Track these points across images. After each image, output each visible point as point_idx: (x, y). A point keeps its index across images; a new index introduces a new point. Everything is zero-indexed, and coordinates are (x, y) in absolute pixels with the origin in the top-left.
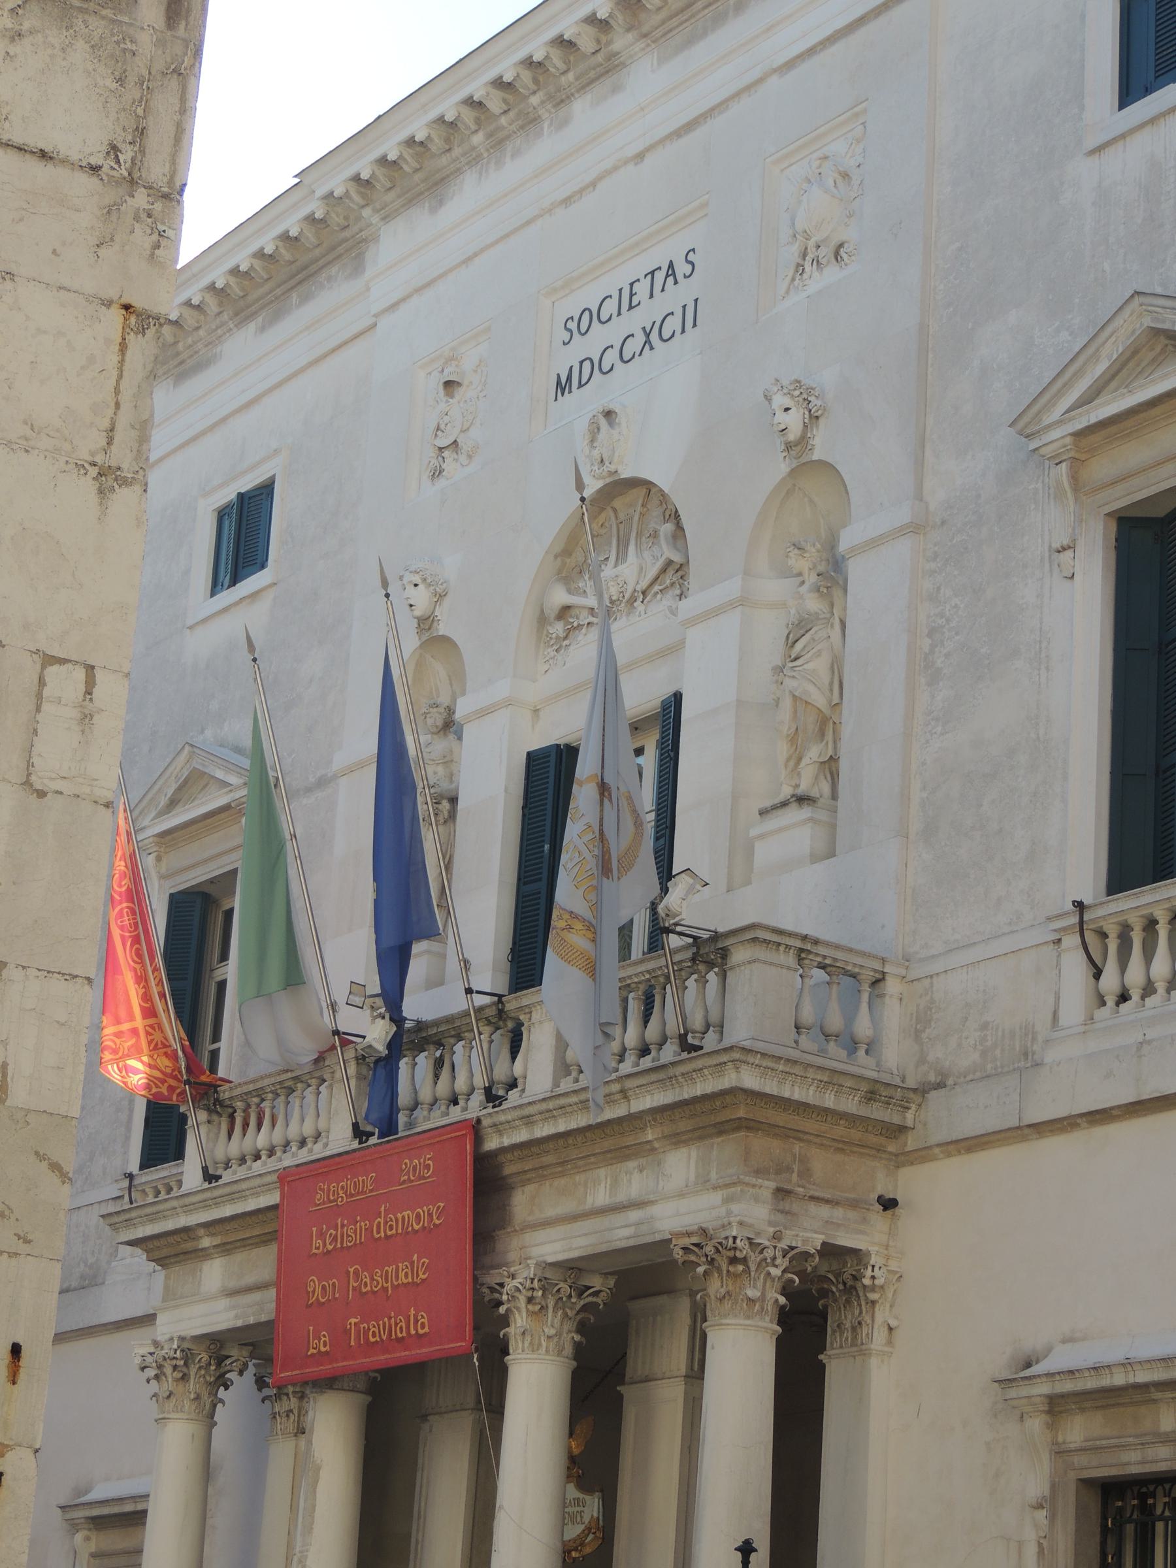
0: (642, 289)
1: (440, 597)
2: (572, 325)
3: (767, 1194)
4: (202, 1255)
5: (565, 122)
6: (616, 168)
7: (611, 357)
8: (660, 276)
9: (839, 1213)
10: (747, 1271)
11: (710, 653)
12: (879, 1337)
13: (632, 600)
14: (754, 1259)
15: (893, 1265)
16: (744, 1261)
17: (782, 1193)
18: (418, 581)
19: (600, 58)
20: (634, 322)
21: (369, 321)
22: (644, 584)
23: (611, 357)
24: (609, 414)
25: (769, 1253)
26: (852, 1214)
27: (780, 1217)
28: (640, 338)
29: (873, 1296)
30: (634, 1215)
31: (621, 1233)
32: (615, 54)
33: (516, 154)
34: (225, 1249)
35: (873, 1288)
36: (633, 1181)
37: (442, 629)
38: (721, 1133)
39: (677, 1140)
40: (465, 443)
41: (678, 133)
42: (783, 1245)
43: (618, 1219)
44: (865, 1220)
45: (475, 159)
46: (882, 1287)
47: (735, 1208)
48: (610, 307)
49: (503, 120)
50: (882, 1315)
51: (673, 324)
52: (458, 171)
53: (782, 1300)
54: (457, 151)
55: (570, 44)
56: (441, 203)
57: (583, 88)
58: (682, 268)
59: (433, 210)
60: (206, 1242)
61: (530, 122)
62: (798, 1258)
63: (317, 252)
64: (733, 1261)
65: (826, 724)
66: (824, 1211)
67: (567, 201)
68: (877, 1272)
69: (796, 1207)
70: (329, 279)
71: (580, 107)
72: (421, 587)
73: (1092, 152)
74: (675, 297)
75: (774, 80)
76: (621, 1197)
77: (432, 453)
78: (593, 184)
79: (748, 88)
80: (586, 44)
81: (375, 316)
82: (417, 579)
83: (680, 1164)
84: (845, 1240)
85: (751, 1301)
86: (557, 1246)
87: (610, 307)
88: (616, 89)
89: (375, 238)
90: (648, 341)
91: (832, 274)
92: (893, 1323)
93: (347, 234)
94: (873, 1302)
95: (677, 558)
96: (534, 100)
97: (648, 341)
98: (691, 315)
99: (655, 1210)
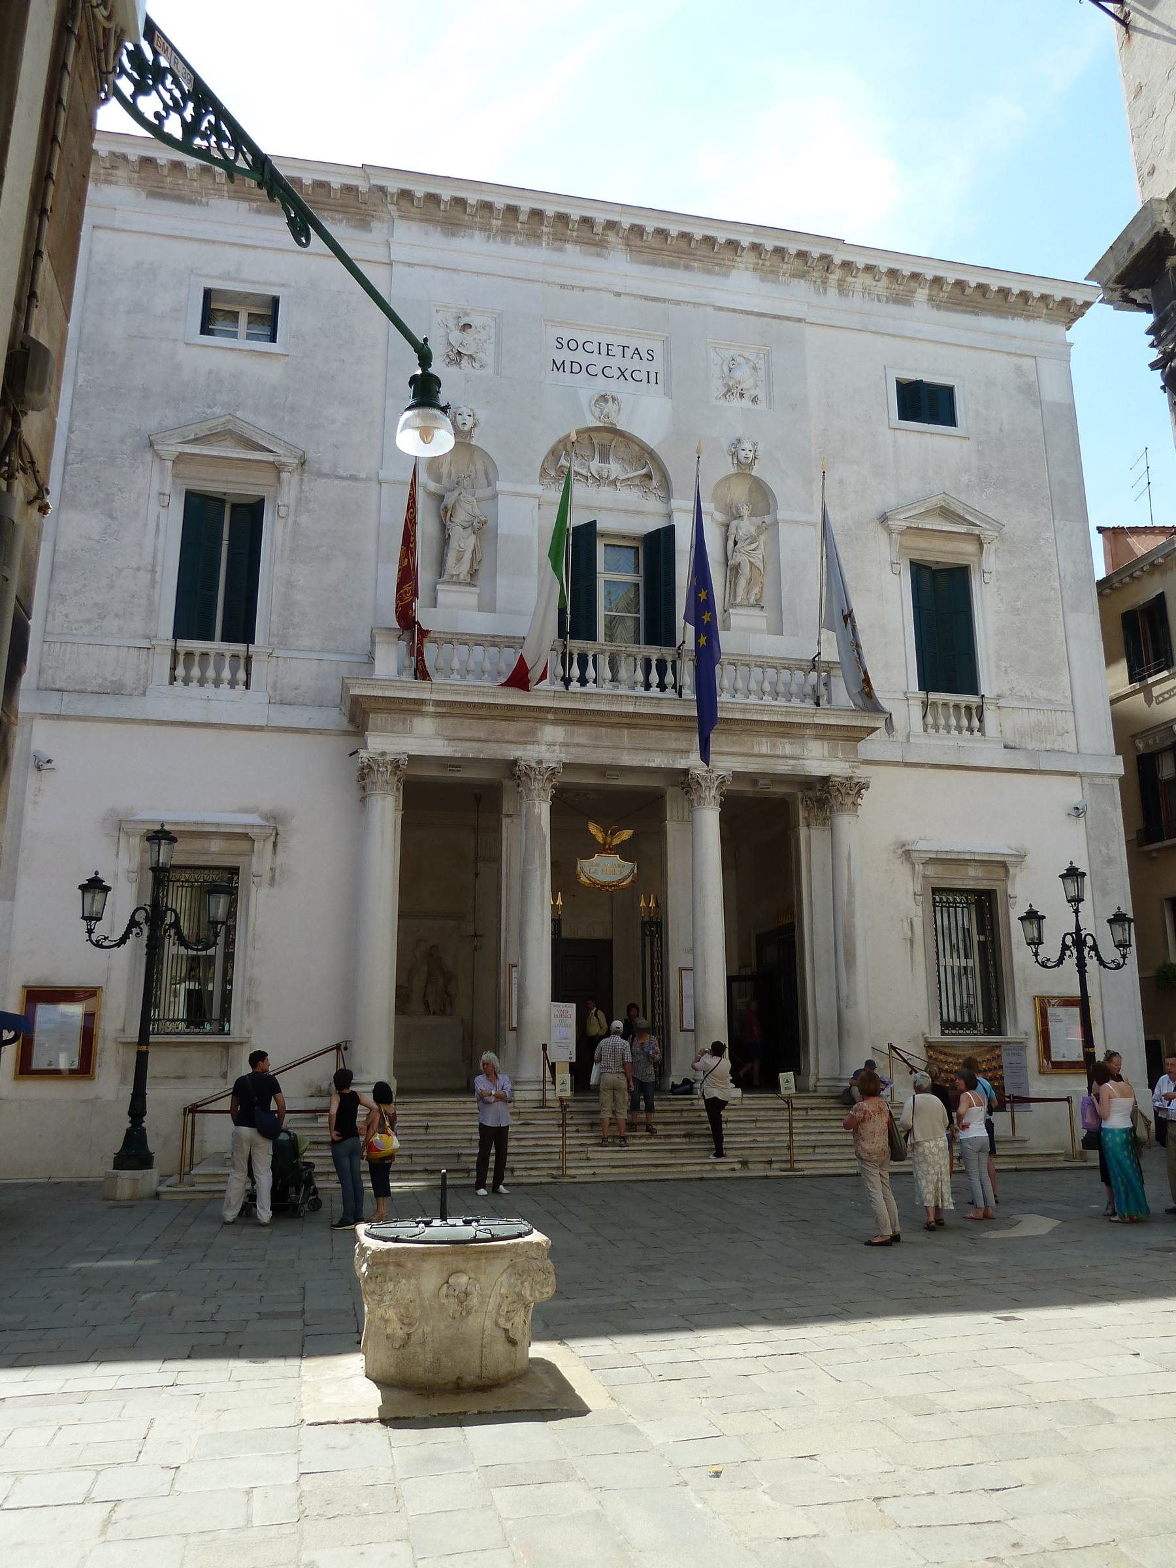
31: (783, 767)
39: (817, 737)
41: (646, 298)
43: (780, 761)
45: (486, 228)
49: (519, 225)
54: (478, 219)
57: (576, 242)
60: (431, 709)
67: (562, 286)
71: (569, 247)
75: (710, 310)
80: (598, 229)
86: (737, 765)
93: (363, 206)
96: (545, 229)
99: (806, 762)
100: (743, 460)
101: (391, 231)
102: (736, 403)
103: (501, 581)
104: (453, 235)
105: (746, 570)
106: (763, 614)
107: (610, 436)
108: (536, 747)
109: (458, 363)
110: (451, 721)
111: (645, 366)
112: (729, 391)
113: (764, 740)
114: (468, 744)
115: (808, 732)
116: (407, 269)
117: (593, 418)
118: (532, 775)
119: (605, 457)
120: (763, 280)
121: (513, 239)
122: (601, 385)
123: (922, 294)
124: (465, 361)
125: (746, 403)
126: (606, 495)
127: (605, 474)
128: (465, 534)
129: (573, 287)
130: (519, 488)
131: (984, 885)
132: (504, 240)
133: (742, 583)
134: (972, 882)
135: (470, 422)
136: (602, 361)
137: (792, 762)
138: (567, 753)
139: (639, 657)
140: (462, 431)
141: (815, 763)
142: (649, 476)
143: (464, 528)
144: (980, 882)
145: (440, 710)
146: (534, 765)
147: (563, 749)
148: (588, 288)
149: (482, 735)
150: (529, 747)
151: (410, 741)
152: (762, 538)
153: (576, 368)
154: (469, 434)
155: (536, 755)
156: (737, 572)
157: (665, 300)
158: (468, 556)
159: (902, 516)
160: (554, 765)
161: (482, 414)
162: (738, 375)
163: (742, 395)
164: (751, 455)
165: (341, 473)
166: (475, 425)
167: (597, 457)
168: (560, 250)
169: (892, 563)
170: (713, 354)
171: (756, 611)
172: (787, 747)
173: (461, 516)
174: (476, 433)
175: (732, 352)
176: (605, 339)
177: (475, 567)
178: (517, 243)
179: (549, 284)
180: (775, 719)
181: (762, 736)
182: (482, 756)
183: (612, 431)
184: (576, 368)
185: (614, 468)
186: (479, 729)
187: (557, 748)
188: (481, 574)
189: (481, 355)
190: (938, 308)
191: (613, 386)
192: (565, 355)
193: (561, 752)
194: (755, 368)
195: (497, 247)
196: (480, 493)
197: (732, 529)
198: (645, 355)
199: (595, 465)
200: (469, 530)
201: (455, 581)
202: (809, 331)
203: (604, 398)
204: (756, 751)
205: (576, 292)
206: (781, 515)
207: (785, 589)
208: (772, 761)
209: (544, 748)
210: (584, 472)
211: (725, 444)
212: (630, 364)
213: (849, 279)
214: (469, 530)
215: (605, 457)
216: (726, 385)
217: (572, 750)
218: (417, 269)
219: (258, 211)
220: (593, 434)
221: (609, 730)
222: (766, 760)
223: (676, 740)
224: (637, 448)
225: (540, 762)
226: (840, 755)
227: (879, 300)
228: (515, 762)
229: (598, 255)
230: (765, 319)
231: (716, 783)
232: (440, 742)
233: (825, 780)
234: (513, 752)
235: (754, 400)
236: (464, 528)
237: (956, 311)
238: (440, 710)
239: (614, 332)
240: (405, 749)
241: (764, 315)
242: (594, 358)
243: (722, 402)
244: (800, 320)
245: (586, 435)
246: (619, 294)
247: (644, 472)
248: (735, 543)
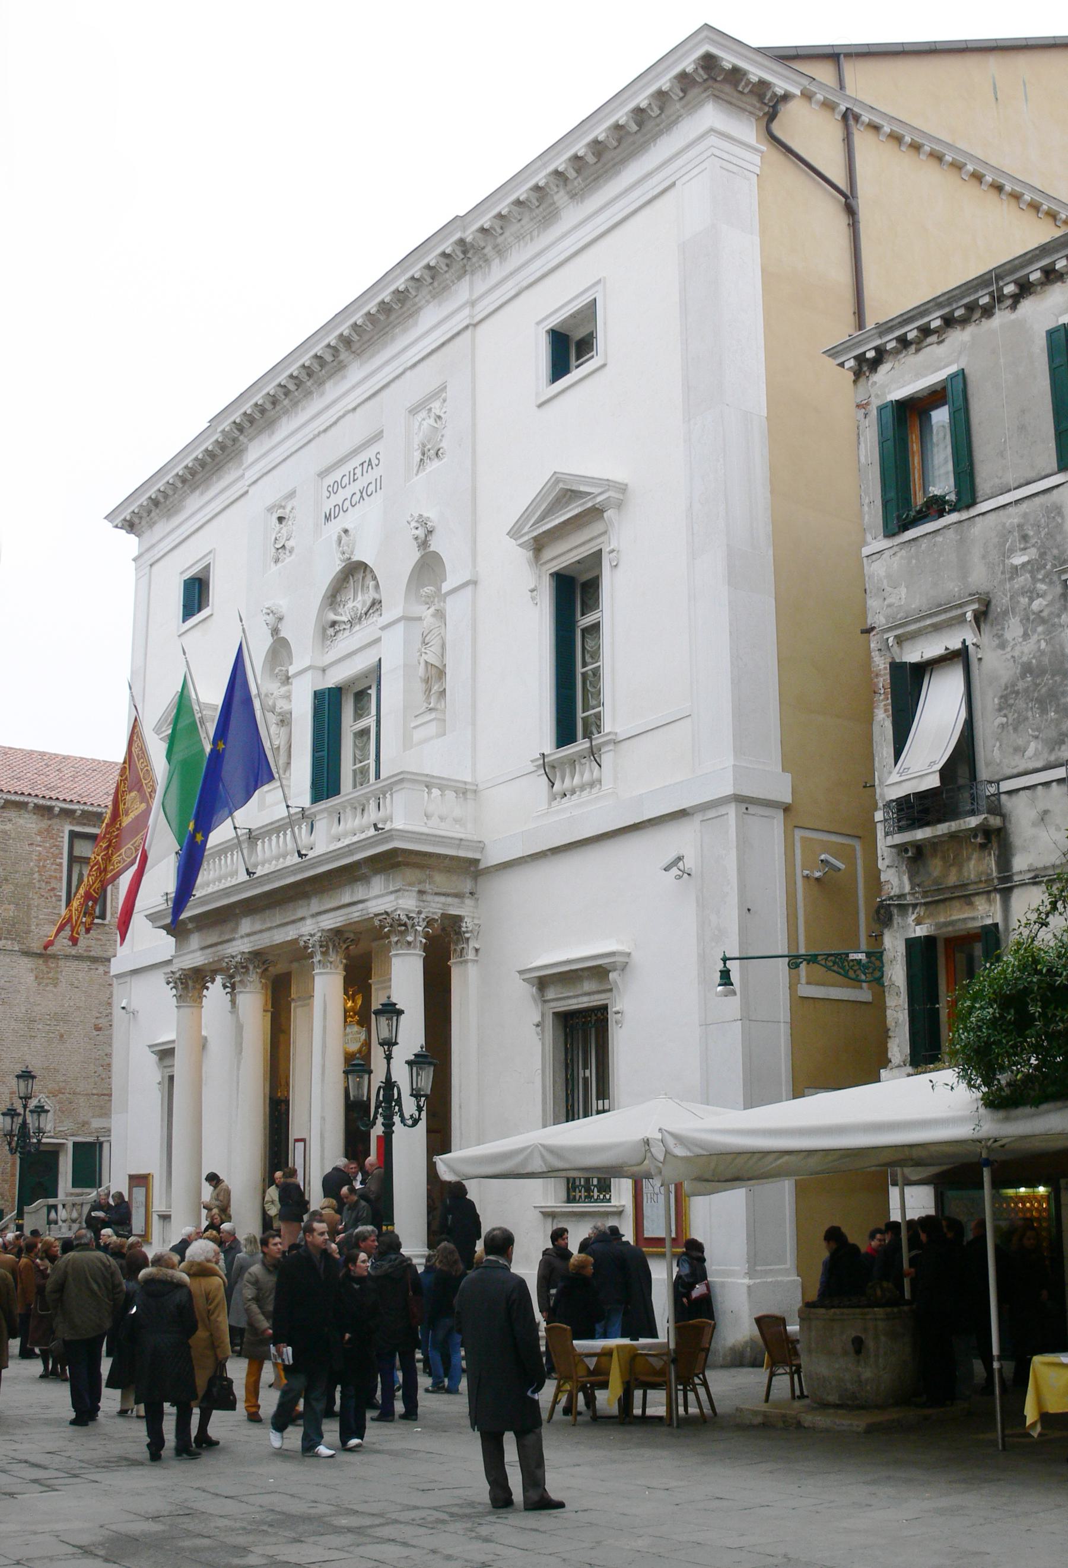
0: (358, 471)
1: (280, 619)
2: (330, 489)
3: (415, 894)
5: (323, 394)
6: (344, 416)
7: (347, 504)
8: (365, 465)
9: (449, 900)
10: (407, 930)
11: (386, 645)
12: (471, 955)
13: (360, 619)
14: (409, 923)
15: (476, 922)
16: (405, 925)
17: (421, 892)
19: (335, 363)
20: (356, 487)
22: (365, 609)
23: (347, 504)
24: (346, 531)
25: (416, 921)
26: (456, 900)
27: (422, 904)
28: (358, 494)
29: (467, 935)
30: (360, 906)
31: (355, 914)
32: (342, 361)
33: (303, 409)
35: (467, 932)
36: (360, 892)
37: (282, 634)
38: (392, 868)
39: (377, 872)
40: (289, 544)
42: (423, 916)
44: (463, 903)
45: (286, 412)
46: (471, 931)
47: (400, 901)
48: (346, 480)
49: (296, 393)
50: (473, 944)
51: (372, 488)
52: (279, 418)
53: (424, 941)
55: (321, 357)
56: (273, 433)
57: (329, 377)
58: (374, 462)
59: (270, 436)
60: (190, 926)
61: (309, 393)
62: (430, 922)
63: (222, 457)
64: (400, 925)
65: (441, 673)
66: (442, 899)
68: (468, 924)
69: (429, 898)
71: (329, 385)
73: (540, 406)
74: (372, 475)
76: (355, 899)
77: (274, 550)
78: (335, 423)
80: (328, 358)
83: (378, 884)
84: (453, 911)
85: (409, 943)
87: (346, 480)
88: (344, 377)
89: (246, 449)
90: (362, 496)
91: (436, 464)
92: (477, 946)
94: (468, 939)
95: (377, 596)
97: (362, 496)
98: (379, 484)
99: (369, 904)
108: (234, 943)
123: (560, 197)
131: (595, 1001)
134: (585, 999)
141: (380, 901)
144: (593, 998)
159: (526, 529)
195: (302, 416)
213: (500, 240)
219: (202, 494)
244: (467, 327)
246: (354, 409)
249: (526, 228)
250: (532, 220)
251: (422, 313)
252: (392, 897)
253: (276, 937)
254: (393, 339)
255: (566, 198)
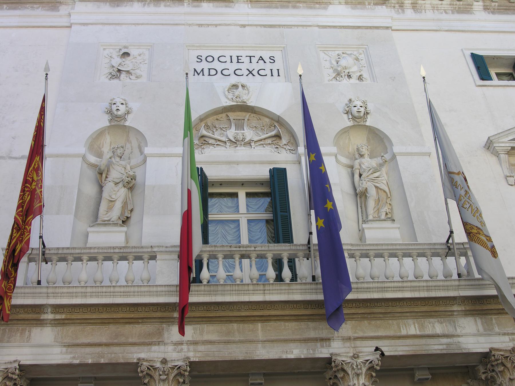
4: (40, 323)
18: (124, 103)
21: (68, 25)
31: (436, 347)
34: (57, 323)
39: (467, 313)
41: (265, 26)
60: (50, 316)
67: (200, 25)
70: (26, 8)
72: (124, 106)
75: (317, 28)
78: (216, 25)
79: (303, 26)
81: (71, 24)
82: (124, 102)
99: (460, 339)
100: (356, 114)
101: (73, 8)
102: (345, 81)
103: (147, 220)
104: (118, 6)
105: (372, 192)
106: (395, 225)
107: (244, 114)
108: (162, 348)
109: (118, 77)
110: (71, 329)
111: (268, 66)
112: (338, 74)
113: (410, 321)
114: (88, 350)
115: (455, 308)
116: (83, 27)
117: (227, 100)
118: (156, 377)
119: (240, 126)
120: (352, 8)
121: (163, 4)
122: (234, 80)
124: (123, 75)
125: (354, 80)
126: (242, 153)
127: (240, 137)
128: (116, 189)
129: (208, 25)
130: (164, 151)
132: (155, 6)
133: (371, 204)
135: (123, 109)
136: (235, 66)
137: (445, 340)
138: (195, 351)
139: (270, 256)
140: (117, 116)
141: (471, 340)
142: (278, 136)
143: (116, 184)
145: (58, 317)
146: (158, 365)
147: (192, 347)
148: (220, 25)
149: (104, 340)
150: (155, 348)
151: (26, 350)
152: (384, 169)
153: (213, 72)
154: (123, 117)
155: (162, 356)
156: (366, 196)
157: (280, 26)
158: (118, 205)
160: (180, 363)
161: (134, 105)
162: (343, 63)
163: (349, 76)
164: (362, 110)
165: (14, 155)
166: (128, 113)
167: (233, 127)
168: (198, 6)
169: (506, 177)
170: (322, 55)
171: (388, 224)
172: (437, 327)
173: (115, 174)
174: (130, 117)
175: (337, 52)
176: (234, 54)
177: (127, 214)
178: (165, 6)
179: (190, 25)
180: (417, 295)
181: (407, 318)
182: (102, 361)
183: (244, 108)
184: (213, 72)
185: (249, 134)
186: (101, 334)
187: (185, 347)
188: (133, 221)
189: (138, 72)
190: (494, 12)
191: (243, 80)
192: (205, 65)
193: (189, 351)
194: (357, 59)
196: (134, 162)
197: (357, 166)
198: (267, 60)
199: (231, 133)
200: (121, 185)
201: (106, 223)
202: (395, 33)
203: (235, 86)
204: (404, 332)
205: (211, 28)
206: (396, 149)
207: (412, 205)
208: (423, 341)
209: (170, 348)
210: (224, 139)
211: (341, 106)
212: (255, 66)
214: (121, 185)
215: (240, 126)
216: (335, 70)
217: (201, 348)
218: (90, 27)
220: (230, 114)
221: (241, 325)
222: (417, 341)
223: (315, 329)
224: (267, 120)
225: (164, 361)
226: (497, 330)
227: (446, 13)
228: (137, 365)
229: (226, 6)
230: (359, 30)
231: (364, 370)
232: (57, 350)
233: (485, 357)
234: (135, 354)
235: (360, 78)
236: (116, 184)
237: (508, 14)
238: (58, 317)
239: (242, 48)
240: (19, 358)
241: (359, 27)
242: (228, 65)
243: (334, 82)
244: (387, 28)
245: (224, 115)
246: (244, 26)
247: (273, 133)
248: (360, 175)
249: (442, 6)
250: (450, 5)
251: (330, 6)
252: (506, 338)
253: (258, 352)
254: (287, 7)
255: (482, 7)
